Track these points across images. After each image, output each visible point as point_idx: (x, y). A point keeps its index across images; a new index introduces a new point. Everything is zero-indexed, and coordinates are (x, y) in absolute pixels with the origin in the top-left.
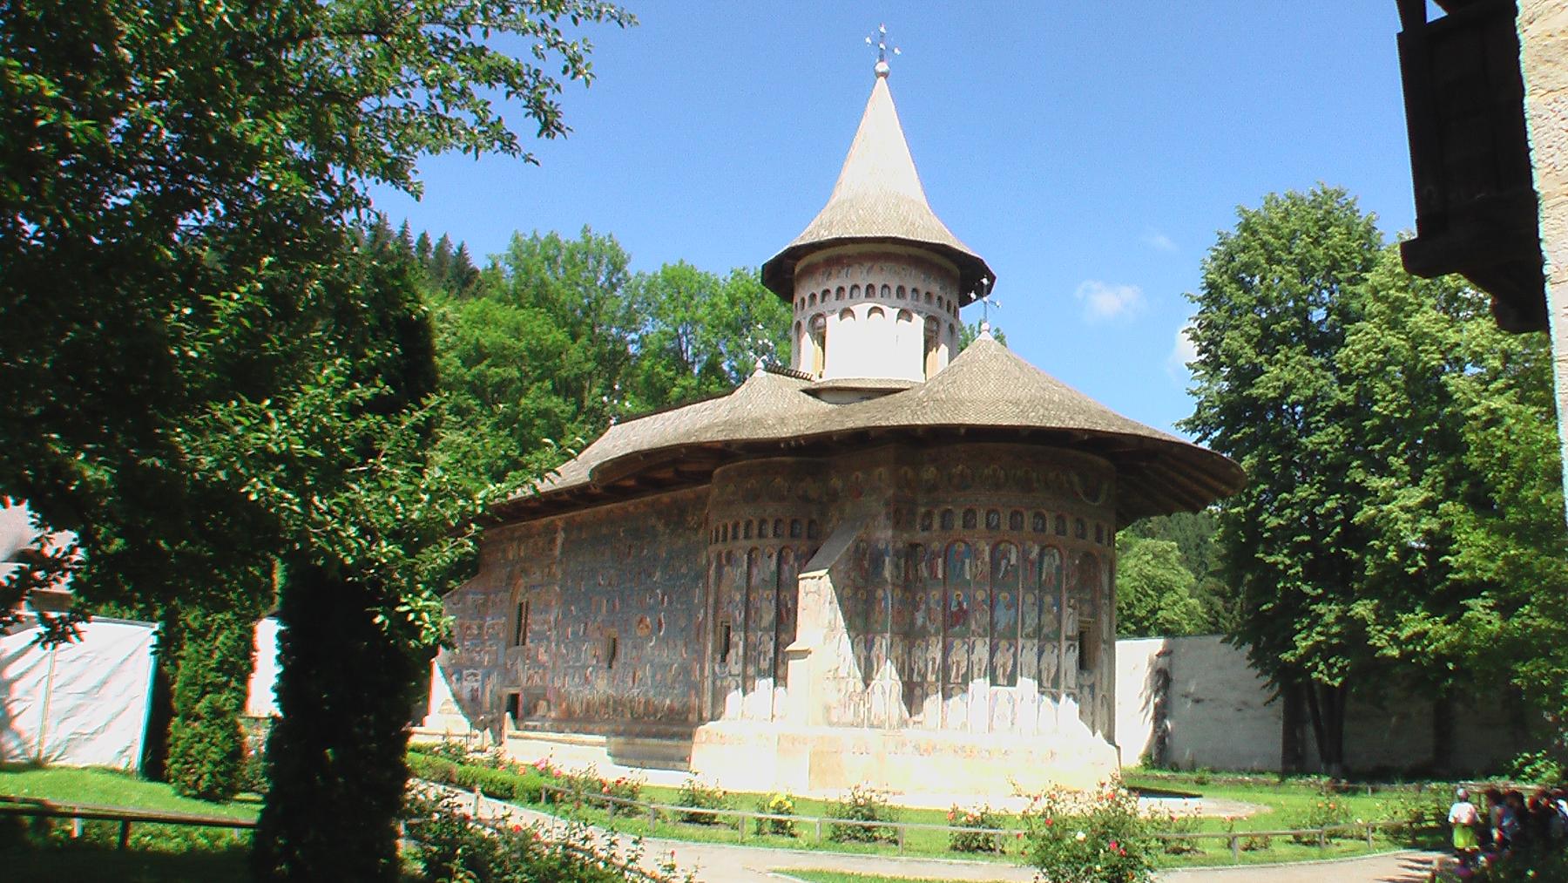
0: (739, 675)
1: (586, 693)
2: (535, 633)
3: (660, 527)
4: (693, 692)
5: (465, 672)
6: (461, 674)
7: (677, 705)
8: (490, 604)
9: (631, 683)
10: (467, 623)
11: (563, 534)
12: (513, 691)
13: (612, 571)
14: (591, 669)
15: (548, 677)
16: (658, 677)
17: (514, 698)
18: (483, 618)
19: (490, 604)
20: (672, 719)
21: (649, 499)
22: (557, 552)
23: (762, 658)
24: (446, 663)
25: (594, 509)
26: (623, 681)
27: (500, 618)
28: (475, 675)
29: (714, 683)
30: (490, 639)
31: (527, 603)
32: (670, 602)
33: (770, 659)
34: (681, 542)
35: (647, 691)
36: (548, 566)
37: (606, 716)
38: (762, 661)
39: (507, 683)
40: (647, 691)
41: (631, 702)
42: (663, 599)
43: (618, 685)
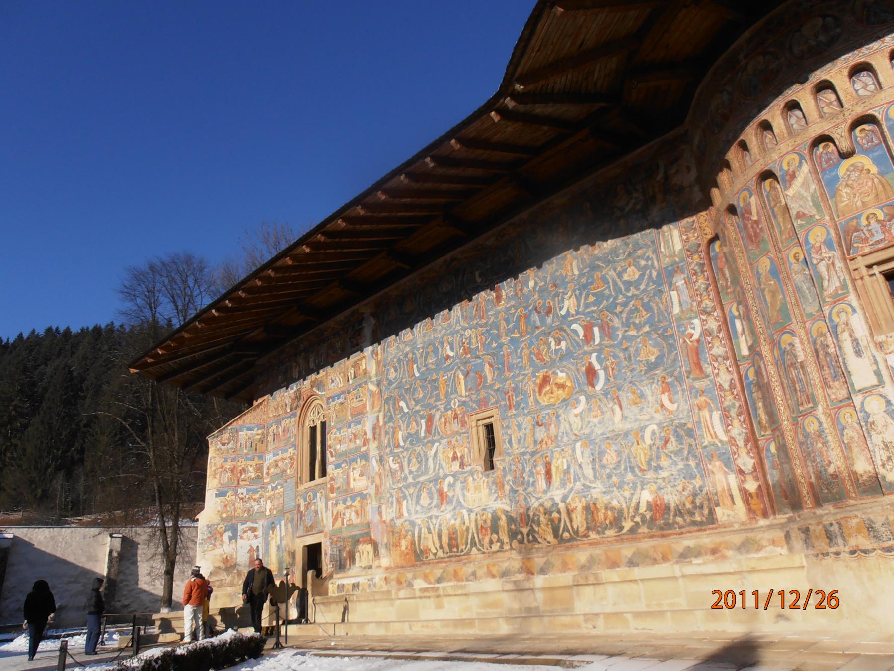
1: (447, 518)
4: (716, 466)
5: (240, 527)
6: (234, 530)
7: (672, 498)
8: (270, 439)
9: (542, 483)
10: (241, 464)
11: (373, 321)
12: (311, 540)
13: (468, 333)
14: (450, 479)
15: (368, 508)
16: (610, 458)
18: (261, 457)
19: (270, 439)
20: (668, 526)
24: (216, 519)
27: (286, 451)
28: (254, 530)
30: (272, 481)
31: (323, 425)
35: (587, 487)
37: (496, 547)
39: (301, 532)
40: (587, 487)
41: (547, 512)
42: (589, 337)
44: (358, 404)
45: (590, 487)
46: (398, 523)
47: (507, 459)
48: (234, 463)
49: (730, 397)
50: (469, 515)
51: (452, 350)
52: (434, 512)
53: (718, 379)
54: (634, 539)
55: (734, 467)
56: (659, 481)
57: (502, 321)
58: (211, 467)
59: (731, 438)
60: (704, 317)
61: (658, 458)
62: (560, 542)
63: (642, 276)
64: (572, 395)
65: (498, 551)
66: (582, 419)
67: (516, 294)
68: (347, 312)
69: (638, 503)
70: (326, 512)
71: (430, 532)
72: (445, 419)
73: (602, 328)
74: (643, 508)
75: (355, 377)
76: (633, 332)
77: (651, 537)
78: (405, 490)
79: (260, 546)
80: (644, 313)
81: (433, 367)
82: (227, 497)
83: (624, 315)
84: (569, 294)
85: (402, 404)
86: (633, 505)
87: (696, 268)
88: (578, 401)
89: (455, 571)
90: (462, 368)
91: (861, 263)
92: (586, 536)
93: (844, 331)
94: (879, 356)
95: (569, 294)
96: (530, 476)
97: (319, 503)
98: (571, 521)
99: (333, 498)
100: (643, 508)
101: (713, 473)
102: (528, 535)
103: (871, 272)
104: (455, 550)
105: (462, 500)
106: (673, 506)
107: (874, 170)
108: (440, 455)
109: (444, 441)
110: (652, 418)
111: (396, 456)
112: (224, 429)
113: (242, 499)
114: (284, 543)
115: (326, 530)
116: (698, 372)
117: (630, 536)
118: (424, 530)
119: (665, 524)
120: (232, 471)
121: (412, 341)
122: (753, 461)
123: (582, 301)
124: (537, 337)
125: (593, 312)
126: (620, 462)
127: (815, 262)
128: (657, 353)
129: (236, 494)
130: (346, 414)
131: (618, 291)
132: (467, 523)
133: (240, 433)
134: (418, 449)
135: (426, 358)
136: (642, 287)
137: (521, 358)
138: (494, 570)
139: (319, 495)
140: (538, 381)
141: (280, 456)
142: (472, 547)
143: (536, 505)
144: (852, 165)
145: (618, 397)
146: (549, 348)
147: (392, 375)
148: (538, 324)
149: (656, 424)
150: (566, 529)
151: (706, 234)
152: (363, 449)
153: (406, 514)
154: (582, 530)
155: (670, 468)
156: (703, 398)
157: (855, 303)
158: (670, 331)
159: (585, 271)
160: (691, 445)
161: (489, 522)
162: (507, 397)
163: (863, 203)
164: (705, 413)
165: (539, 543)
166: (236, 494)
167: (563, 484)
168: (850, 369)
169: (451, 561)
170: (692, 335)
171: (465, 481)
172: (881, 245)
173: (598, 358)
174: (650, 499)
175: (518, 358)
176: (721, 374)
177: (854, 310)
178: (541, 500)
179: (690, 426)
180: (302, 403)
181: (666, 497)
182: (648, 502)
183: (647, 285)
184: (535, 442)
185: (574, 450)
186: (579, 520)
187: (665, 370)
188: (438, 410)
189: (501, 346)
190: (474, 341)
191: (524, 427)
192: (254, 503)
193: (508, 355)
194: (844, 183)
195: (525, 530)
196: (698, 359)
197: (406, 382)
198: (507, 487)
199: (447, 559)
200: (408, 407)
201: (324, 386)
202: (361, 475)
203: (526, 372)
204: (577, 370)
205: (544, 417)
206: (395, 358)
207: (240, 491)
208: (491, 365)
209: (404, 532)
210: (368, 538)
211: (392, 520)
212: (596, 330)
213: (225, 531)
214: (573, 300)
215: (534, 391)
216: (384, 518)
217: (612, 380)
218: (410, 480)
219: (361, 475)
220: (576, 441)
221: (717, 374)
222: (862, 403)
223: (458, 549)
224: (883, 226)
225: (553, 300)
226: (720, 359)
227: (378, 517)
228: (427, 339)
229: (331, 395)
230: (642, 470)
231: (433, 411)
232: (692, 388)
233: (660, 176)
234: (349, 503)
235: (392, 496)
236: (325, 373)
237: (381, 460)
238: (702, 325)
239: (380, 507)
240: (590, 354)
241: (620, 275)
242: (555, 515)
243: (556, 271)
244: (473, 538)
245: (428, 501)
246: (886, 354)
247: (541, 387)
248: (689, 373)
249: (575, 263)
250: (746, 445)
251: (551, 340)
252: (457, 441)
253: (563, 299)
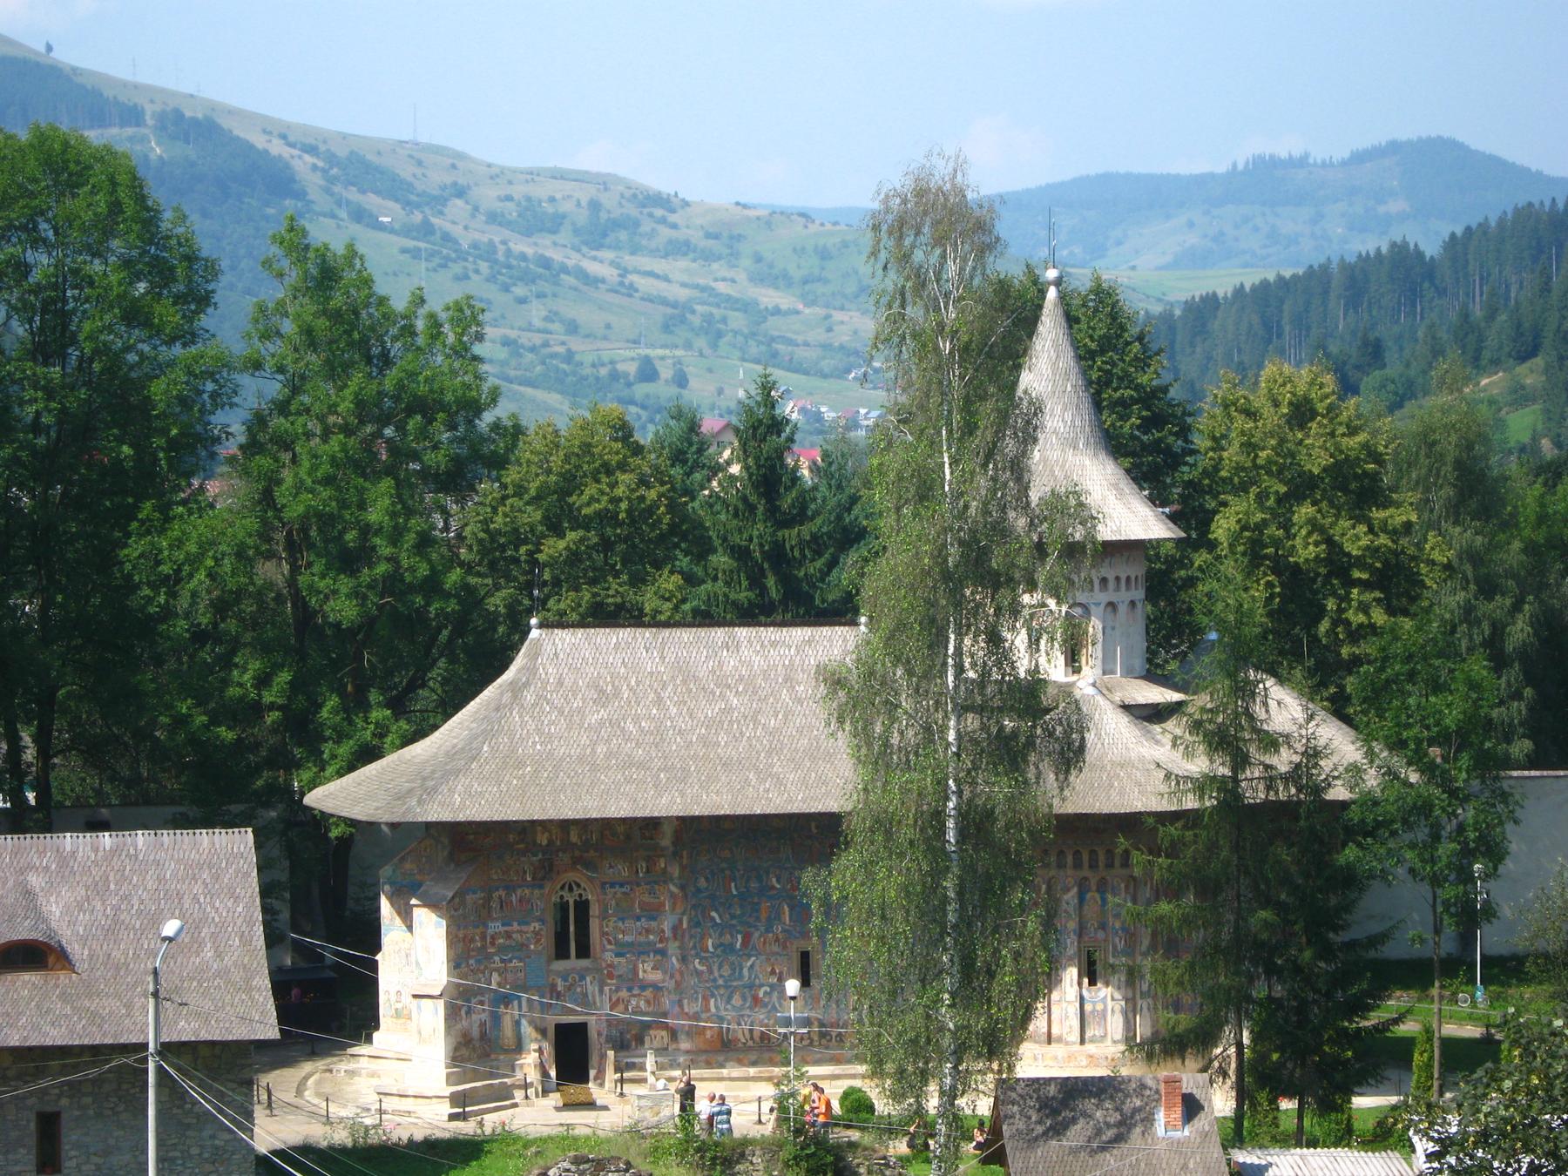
51: (778, 881)
52: (748, 1012)
85: (714, 914)
108: (757, 968)
153: (713, 1010)
200: (720, 917)
216: (686, 1010)
218: (721, 982)
235: (696, 992)
237: (684, 959)
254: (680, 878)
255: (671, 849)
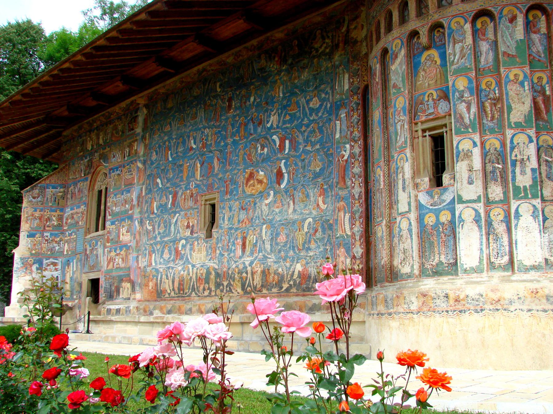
0: (478, 200)
2: (113, 214)
3: (273, 66)
5: (45, 262)
6: (41, 263)
9: (239, 252)
10: (47, 214)
11: (145, 111)
12: (93, 276)
13: (207, 131)
14: (183, 242)
15: (130, 257)
16: (282, 238)
17: (95, 284)
18: (62, 210)
21: (254, 42)
22: (139, 130)
23: (518, 170)
24: (27, 254)
25: (183, 75)
26: (229, 250)
27: (79, 207)
28: (55, 264)
29: (420, 219)
31: (106, 188)
32: (294, 146)
33: (533, 170)
34: (305, 75)
35: (265, 257)
36: (130, 146)
37: (207, 293)
38: (519, 177)
39: (86, 270)
40: (265, 257)
41: (240, 273)
42: (282, 147)
43: (222, 255)
44: (130, 177)
45: (267, 257)
46: (149, 269)
47: (220, 231)
48: (42, 213)
49: (357, 205)
50: (193, 269)
51: (195, 143)
52: (171, 265)
53: (353, 191)
54: (287, 296)
55: (351, 254)
56: (308, 258)
57: (230, 126)
58: (24, 215)
59: (353, 233)
60: (353, 144)
61: (310, 242)
62: (244, 294)
63: (321, 105)
64: (266, 189)
65: (208, 296)
66: (269, 208)
67: (241, 106)
68: (128, 101)
69: (294, 272)
70: (103, 256)
71: (167, 279)
72: (185, 196)
73: (290, 142)
74: (295, 276)
75: (129, 155)
76: (309, 148)
77: (297, 295)
78: (154, 246)
79: (59, 276)
80: (318, 134)
81: (181, 155)
82: (35, 238)
83: (306, 134)
84: (275, 111)
85: (159, 181)
86: (290, 273)
87: (354, 106)
88: (269, 195)
89: (179, 306)
90: (200, 158)
91: (420, 127)
92: (260, 291)
93: (400, 173)
94: (413, 193)
95: (275, 111)
96: (232, 246)
97: (99, 250)
98: (253, 280)
99: (108, 247)
100: (295, 276)
101: (339, 256)
102: (227, 287)
103: (425, 134)
104: (182, 292)
105: (189, 258)
106: (313, 276)
107: (439, 62)
108: (179, 223)
109: (182, 213)
110: (311, 213)
111: (151, 220)
112: (35, 186)
113: (47, 240)
114: (75, 275)
115: (103, 270)
116: (342, 184)
117: (285, 294)
118: (164, 277)
119: (306, 288)
120: (40, 219)
121: (169, 131)
122: (362, 250)
123: (282, 118)
124: (250, 142)
125: (287, 128)
126: (287, 242)
127: (396, 121)
128: (321, 166)
129: (43, 236)
130: (121, 183)
131: (305, 115)
132: (191, 274)
133: (47, 190)
134: (166, 217)
135: (177, 147)
136: (320, 114)
137: (238, 156)
138: (203, 308)
139: (99, 243)
140: (247, 176)
141: (76, 210)
142: (192, 291)
143: (234, 266)
144: (429, 55)
145: (293, 195)
146: (257, 151)
147: (154, 157)
148: (252, 131)
149: (312, 218)
150: (249, 285)
151: (364, 81)
152: (130, 212)
153: (154, 264)
154: (258, 286)
155: (315, 250)
156: (342, 203)
157: (408, 155)
158: (331, 151)
159: (287, 95)
160: (329, 236)
161: (204, 275)
162: (225, 185)
163: (429, 84)
164: (342, 214)
165: (233, 293)
166: (43, 236)
167: (252, 254)
168: (399, 198)
169: (178, 300)
170: (344, 156)
171: (192, 244)
172: (431, 117)
173: (285, 164)
174: (301, 270)
175: (236, 156)
176: (355, 187)
177: (407, 160)
178: (237, 263)
179: (331, 222)
180: (92, 170)
181: (310, 269)
182: (299, 272)
183: (323, 114)
184: (239, 221)
185: (261, 230)
186: (257, 280)
187: (324, 179)
188: (181, 188)
189: (226, 145)
190: (210, 138)
191: (233, 209)
192: (55, 245)
193: (231, 153)
194: (423, 68)
195: (225, 283)
196: (344, 174)
197: (163, 164)
198: (218, 252)
199: (176, 298)
200: (162, 183)
201: (108, 159)
202: (127, 232)
203: (240, 168)
204: (272, 171)
205: (246, 203)
206: (157, 144)
207: (45, 234)
208: (218, 160)
209: (151, 276)
210: (129, 279)
211: (145, 267)
212: (287, 142)
213: (34, 263)
214: (276, 117)
215: (243, 183)
216: (140, 265)
217: (291, 181)
218: (159, 239)
219: (127, 232)
220: (263, 224)
221: (353, 187)
222: (400, 222)
223: (184, 292)
224: (435, 103)
225: (264, 114)
226: (357, 176)
227: (136, 264)
228: (179, 131)
229: (112, 167)
230: (299, 249)
231: (178, 189)
232: (337, 194)
233: (344, 30)
234: (118, 252)
236: (109, 149)
237: (141, 223)
238: (351, 149)
239: (138, 257)
240: (282, 160)
241: (308, 102)
242: (244, 275)
243: (269, 91)
244: (193, 285)
245: (168, 256)
246: (418, 192)
247: (248, 180)
248: (338, 183)
249: (281, 87)
250: (360, 239)
251: (259, 145)
252: (191, 214)
253: (270, 114)
254: (144, 155)
255: (142, 134)
